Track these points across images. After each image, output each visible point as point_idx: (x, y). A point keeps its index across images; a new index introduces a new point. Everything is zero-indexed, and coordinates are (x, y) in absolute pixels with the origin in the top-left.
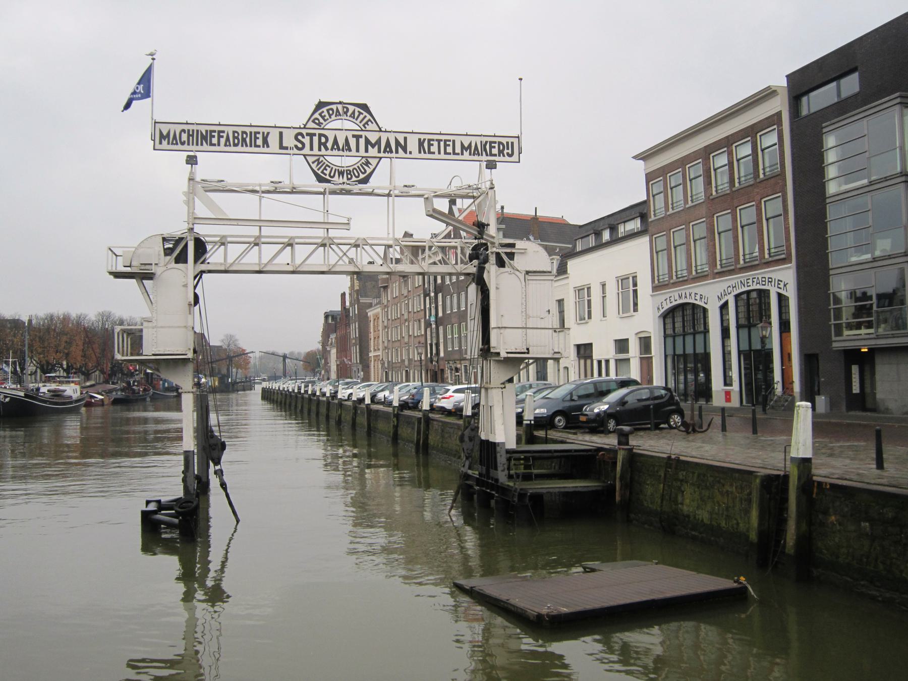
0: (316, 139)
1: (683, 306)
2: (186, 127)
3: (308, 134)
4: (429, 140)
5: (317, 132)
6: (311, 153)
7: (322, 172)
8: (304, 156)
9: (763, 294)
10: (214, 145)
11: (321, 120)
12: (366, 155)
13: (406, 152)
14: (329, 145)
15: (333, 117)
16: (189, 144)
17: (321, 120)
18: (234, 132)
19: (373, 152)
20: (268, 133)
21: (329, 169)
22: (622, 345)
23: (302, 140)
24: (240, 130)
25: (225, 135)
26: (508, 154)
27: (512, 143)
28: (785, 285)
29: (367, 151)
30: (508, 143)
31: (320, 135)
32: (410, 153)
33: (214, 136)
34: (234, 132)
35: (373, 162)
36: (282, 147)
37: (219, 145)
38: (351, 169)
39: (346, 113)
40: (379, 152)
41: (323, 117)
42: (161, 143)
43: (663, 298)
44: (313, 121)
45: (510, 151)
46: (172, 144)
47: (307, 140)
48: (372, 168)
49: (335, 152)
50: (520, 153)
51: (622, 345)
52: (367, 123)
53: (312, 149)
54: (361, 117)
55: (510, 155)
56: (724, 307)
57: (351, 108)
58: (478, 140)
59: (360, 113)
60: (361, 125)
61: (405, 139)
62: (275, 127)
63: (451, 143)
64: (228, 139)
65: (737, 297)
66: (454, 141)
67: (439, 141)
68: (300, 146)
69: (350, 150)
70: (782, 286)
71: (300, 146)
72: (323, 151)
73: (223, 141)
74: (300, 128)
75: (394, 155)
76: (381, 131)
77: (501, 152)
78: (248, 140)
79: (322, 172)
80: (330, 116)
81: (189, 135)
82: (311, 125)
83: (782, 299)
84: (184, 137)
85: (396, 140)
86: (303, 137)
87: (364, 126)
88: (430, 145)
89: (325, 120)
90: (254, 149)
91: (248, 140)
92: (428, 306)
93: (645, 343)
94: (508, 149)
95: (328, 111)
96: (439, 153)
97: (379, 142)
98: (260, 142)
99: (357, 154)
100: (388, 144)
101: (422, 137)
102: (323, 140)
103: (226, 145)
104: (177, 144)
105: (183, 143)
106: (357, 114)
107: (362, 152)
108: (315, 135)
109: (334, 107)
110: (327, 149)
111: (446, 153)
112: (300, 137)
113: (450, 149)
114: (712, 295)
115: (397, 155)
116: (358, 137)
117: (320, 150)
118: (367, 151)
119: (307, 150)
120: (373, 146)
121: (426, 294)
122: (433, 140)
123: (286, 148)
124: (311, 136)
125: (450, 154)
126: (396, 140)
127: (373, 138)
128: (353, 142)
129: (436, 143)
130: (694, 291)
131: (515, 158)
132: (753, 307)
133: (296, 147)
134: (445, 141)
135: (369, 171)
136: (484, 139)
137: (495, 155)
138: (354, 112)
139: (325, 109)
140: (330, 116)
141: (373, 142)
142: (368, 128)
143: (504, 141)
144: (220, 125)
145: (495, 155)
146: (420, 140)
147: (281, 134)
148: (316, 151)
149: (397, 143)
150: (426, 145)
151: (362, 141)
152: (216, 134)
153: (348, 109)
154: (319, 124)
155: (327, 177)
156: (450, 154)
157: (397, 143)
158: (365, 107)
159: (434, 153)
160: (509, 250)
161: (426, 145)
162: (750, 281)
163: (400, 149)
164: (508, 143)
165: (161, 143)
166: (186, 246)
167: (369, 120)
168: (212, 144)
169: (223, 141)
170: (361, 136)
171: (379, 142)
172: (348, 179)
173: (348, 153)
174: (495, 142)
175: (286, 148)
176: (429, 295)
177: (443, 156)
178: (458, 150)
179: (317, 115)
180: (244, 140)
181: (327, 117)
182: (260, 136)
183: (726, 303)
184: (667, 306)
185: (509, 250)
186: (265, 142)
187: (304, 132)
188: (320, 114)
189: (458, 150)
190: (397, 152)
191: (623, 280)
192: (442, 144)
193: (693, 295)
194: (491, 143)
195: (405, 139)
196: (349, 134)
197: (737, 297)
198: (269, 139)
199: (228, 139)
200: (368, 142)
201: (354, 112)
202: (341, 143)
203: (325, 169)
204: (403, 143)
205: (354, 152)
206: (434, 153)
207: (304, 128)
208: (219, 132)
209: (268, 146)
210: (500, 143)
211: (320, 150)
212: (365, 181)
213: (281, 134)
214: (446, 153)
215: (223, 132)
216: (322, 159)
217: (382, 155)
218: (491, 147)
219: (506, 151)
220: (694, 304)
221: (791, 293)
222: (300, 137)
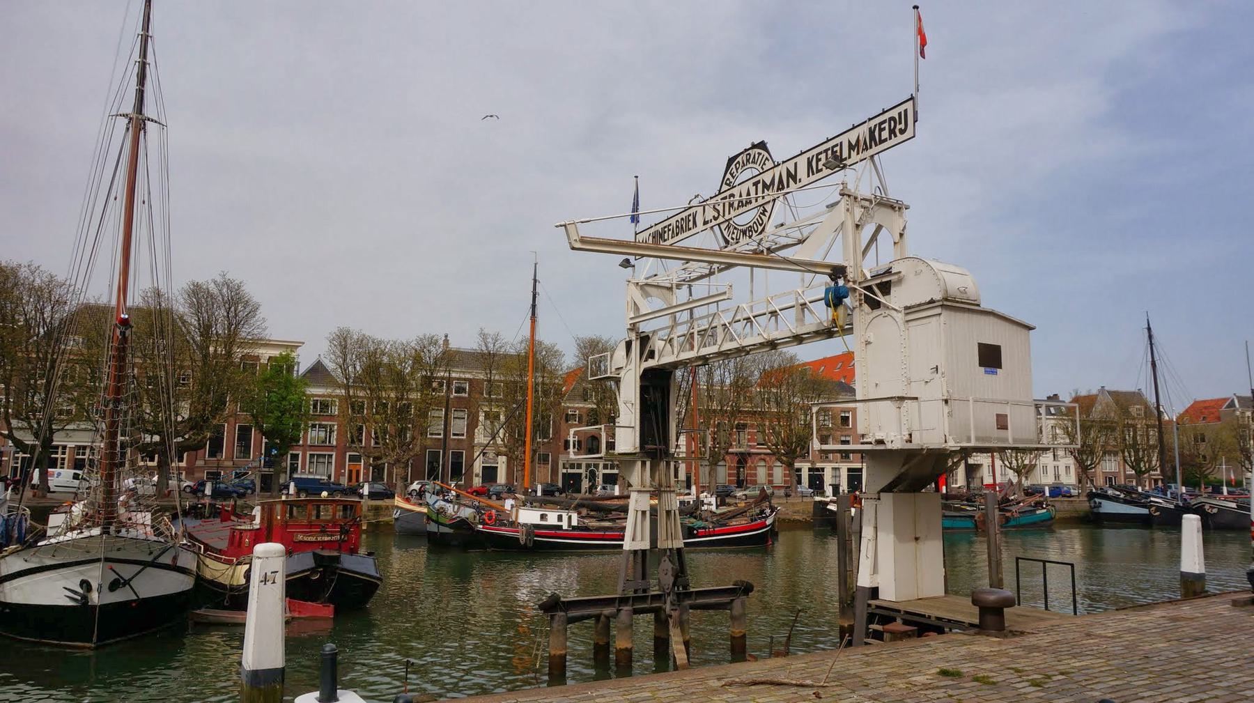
27: (906, 111)
35: (768, 207)
45: (902, 126)
50: (915, 121)
75: (786, 190)
98: (691, 224)
101: (809, 155)
116: (756, 184)
119: (721, 219)
137: (885, 140)
142: (765, 168)
143: (894, 113)
151: (760, 186)
179: (728, 176)
186: (695, 224)
219: (898, 127)
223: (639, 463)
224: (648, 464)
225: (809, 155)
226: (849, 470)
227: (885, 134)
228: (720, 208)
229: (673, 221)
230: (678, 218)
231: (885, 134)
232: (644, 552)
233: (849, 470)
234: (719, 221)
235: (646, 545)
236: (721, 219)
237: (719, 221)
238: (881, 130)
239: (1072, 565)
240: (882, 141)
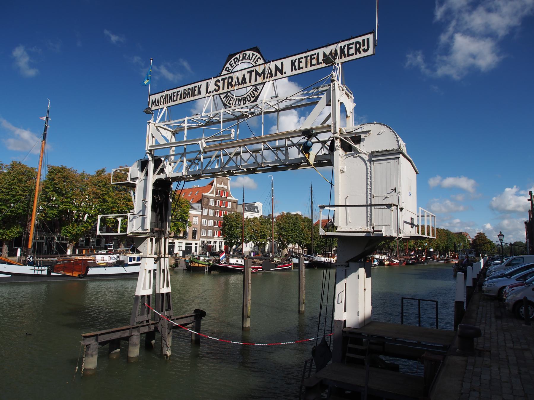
0: (226, 81)
5: (227, 76)
8: (219, 95)
12: (256, 83)
13: (282, 74)
19: (260, 80)
23: (219, 84)
25: (180, 93)
27: (368, 39)
31: (229, 78)
32: (285, 73)
38: (246, 96)
40: (264, 79)
41: (231, 65)
44: (226, 70)
45: (365, 47)
47: (221, 84)
48: (259, 91)
53: (223, 89)
55: (365, 51)
57: (248, 53)
59: (253, 55)
61: (282, 63)
63: (315, 56)
67: (306, 57)
68: (217, 88)
69: (246, 83)
71: (217, 88)
72: (230, 89)
75: (274, 78)
77: (357, 51)
78: (191, 93)
85: (276, 66)
86: (219, 82)
89: (232, 67)
91: (191, 93)
94: (364, 45)
95: (234, 60)
98: (196, 93)
102: (230, 80)
103: (180, 99)
106: (251, 56)
108: (226, 78)
109: (238, 56)
110: (232, 86)
112: (217, 83)
113: (314, 62)
116: (250, 72)
118: (256, 80)
119: (221, 91)
122: (302, 58)
125: (314, 65)
126: (276, 66)
127: (260, 69)
129: (304, 60)
133: (215, 90)
137: (352, 55)
139: (232, 60)
140: (235, 62)
142: (258, 63)
145: (352, 55)
146: (292, 61)
147: (207, 83)
149: (276, 67)
151: (253, 74)
152: (176, 94)
153: (246, 54)
156: (314, 65)
157: (276, 67)
159: (302, 68)
163: (278, 73)
167: (259, 58)
168: (174, 101)
169: (179, 97)
170: (253, 71)
172: (244, 104)
174: (352, 44)
175: (210, 92)
179: (228, 65)
180: (189, 93)
181: (234, 64)
182: (196, 89)
186: (199, 92)
187: (220, 78)
188: (230, 64)
190: (276, 75)
194: (349, 45)
195: (282, 63)
198: (201, 89)
203: (231, 100)
206: (302, 68)
207: (221, 76)
210: (356, 43)
213: (207, 83)
214: (311, 65)
215: (179, 91)
218: (349, 49)
219: (362, 48)
222: (217, 83)
223: (149, 239)
224: (154, 239)
225: (293, 58)
226: (187, 244)
227: (352, 51)
228: (221, 84)
229: (181, 89)
230: (186, 88)
231: (352, 51)
232: (149, 296)
233: (187, 244)
234: (218, 92)
235: (150, 292)
236: (221, 91)
237: (218, 92)
238: (349, 49)
239: (437, 302)
240: (349, 55)
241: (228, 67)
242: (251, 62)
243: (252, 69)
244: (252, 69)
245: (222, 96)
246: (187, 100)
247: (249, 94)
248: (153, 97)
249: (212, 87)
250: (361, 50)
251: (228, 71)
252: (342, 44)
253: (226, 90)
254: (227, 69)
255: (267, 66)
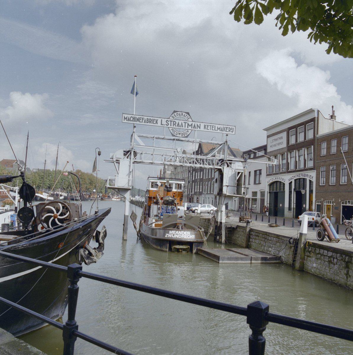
0: (172, 123)
1: (277, 182)
2: (133, 116)
3: (170, 121)
4: (207, 125)
6: (171, 127)
7: (174, 133)
9: (304, 180)
10: (141, 122)
11: (174, 117)
14: (176, 125)
15: (178, 116)
16: (133, 121)
17: (174, 117)
18: (147, 119)
19: (190, 128)
20: (158, 120)
21: (176, 132)
22: (255, 194)
24: (149, 118)
25: (144, 119)
26: (231, 131)
27: (233, 128)
28: (312, 177)
29: (188, 127)
30: (232, 128)
31: (174, 121)
33: (141, 119)
34: (147, 119)
35: (190, 131)
36: (162, 124)
37: (142, 122)
39: (182, 115)
40: (192, 128)
41: (175, 116)
42: (124, 120)
43: (269, 179)
44: (172, 117)
45: (232, 131)
46: (128, 121)
47: (169, 123)
48: (189, 133)
49: (178, 127)
51: (255, 194)
52: (188, 119)
53: (171, 125)
54: (187, 116)
56: (290, 184)
57: (184, 114)
58: (222, 126)
59: (186, 115)
60: (187, 119)
61: (200, 124)
62: (160, 118)
63: (214, 127)
64: (145, 121)
65: (295, 180)
66: (215, 126)
67: (210, 126)
69: (183, 127)
70: (311, 177)
72: (174, 127)
73: (143, 121)
74: (168, 119)
75: (196, 129)
76: (192, 121)
77: (229, 131)
79: (174, 133)
80: (177, 115)
81: (133, 118)
82: (171, 118)
83: (311, 182)
84: (132, 119)
86: (169, 122)
87: (187, 119)
88: (207, 127)
89: (176, 117)
90: (153, 124)
92: (189, 176)
93: (263, 194)
94: (232, 130)
95: (177, 114)
96: (210, 130)
97: (192, 125)
98: (155, 122)
99: (185, 128)
100: (195, 125)
101: (205, 124)
102: (175, 123)
103: (144, 122)
104: (129, 121)
105: (131, 121)
106: (185, 115)
107: (186, 128)
108: (172, 121)
109: (179, 113)
110: (176, 126)
111: (212, 130)
112: (167, 122)
113: (214, 129)
114: (287, 179)
115: (197, 130)
116: (185, 123)
117: (173, 126)
118: (188, 127)
119: (169, 126)
120: (190, 126)
121: (189, 172)
123: (163, 125)
124: (171, 121)
125: (213, 130)
127: (190, 123)
128: (184, 124)
129: (209, 126)
130: (281, 177)
131: (234, 133)
132: (300, 183)
133: (166, 124)
134: (212, 126)
135: (188, 134)
136: (225, 126)
138: (184, 115)
139: (176, 113)
140: (177, 115)
141: (190, 124)
143: (231, 127)
144: (143, 116)
147: (162, 120)
148: (172, 126)
149: (198, 126)
150: (206, 127)
152: (141, 119)
154: (174, 118)
155: (175, 135)
156: (213, 130)
157: (198, 126)
158: (188, 113)
159: (209, 129)
160: (230, 162)
161: (206, 127)
162: (300, 175)
164: (232, 128)
165: (124, 120)
166: (131, 153)
167: (189, 118)
168: (140, 122)
169: (143, 121)
170: (186, 123)
171: (192, 125)
172: (182, 136)
173: (182, 128)
175: (163, 125)
176: (190, 172)
177: (211, 131)
178: (216, 129)
179: (173, 115)
181: (176, 116)
183: (291, 182)
184: (271, 181)
185: (230, 162)
186: (157, 122)
187: (169, 120)
188: (174, 115)
189: (216, 129)
190: (197, 128)
191: (255, 171)
192: (211, 127)
193: (280, 178)
194: (227, 127)
195: (200, 124)
196: (183, 122)
197: (295, 180)
198: (158, 122)
199: (145, 121)
200: (188, 124)
201: (184, 115)
202: (180, 124)
204: (199, 125)
205: (184, 128)
206: (209, 129)
208: (143, 118)
209: (157, 124)
210: (229, 128)
211: (173, 126)
212: (187, 137)
213: (162, 120)
214: (212, 130)
215: (144, 118)
216: (174, 129)
217: (193, 129)
218: (226, 129)
220: (280, 182)
221: (314, 180)
222: (167, 122)
225: (205, 124)
227: (228, 130)
228: (169, 123)
229: (146, 118)
231: (228, 130)
234: (168, 126)
237: (168, 126)
241: (173, 116)
242: (186, 118)
243: (186, 122)
244: (186, 122)
245: (170, 129)
246: (148, 124)
247: (184, 132)
248: (126, 116)
249: (164, 122)
250: (231, 131)
251: (174, 118)
252: (225, 126)
253: (172, 126)
254: (173, 117)
255: (194, 123)
